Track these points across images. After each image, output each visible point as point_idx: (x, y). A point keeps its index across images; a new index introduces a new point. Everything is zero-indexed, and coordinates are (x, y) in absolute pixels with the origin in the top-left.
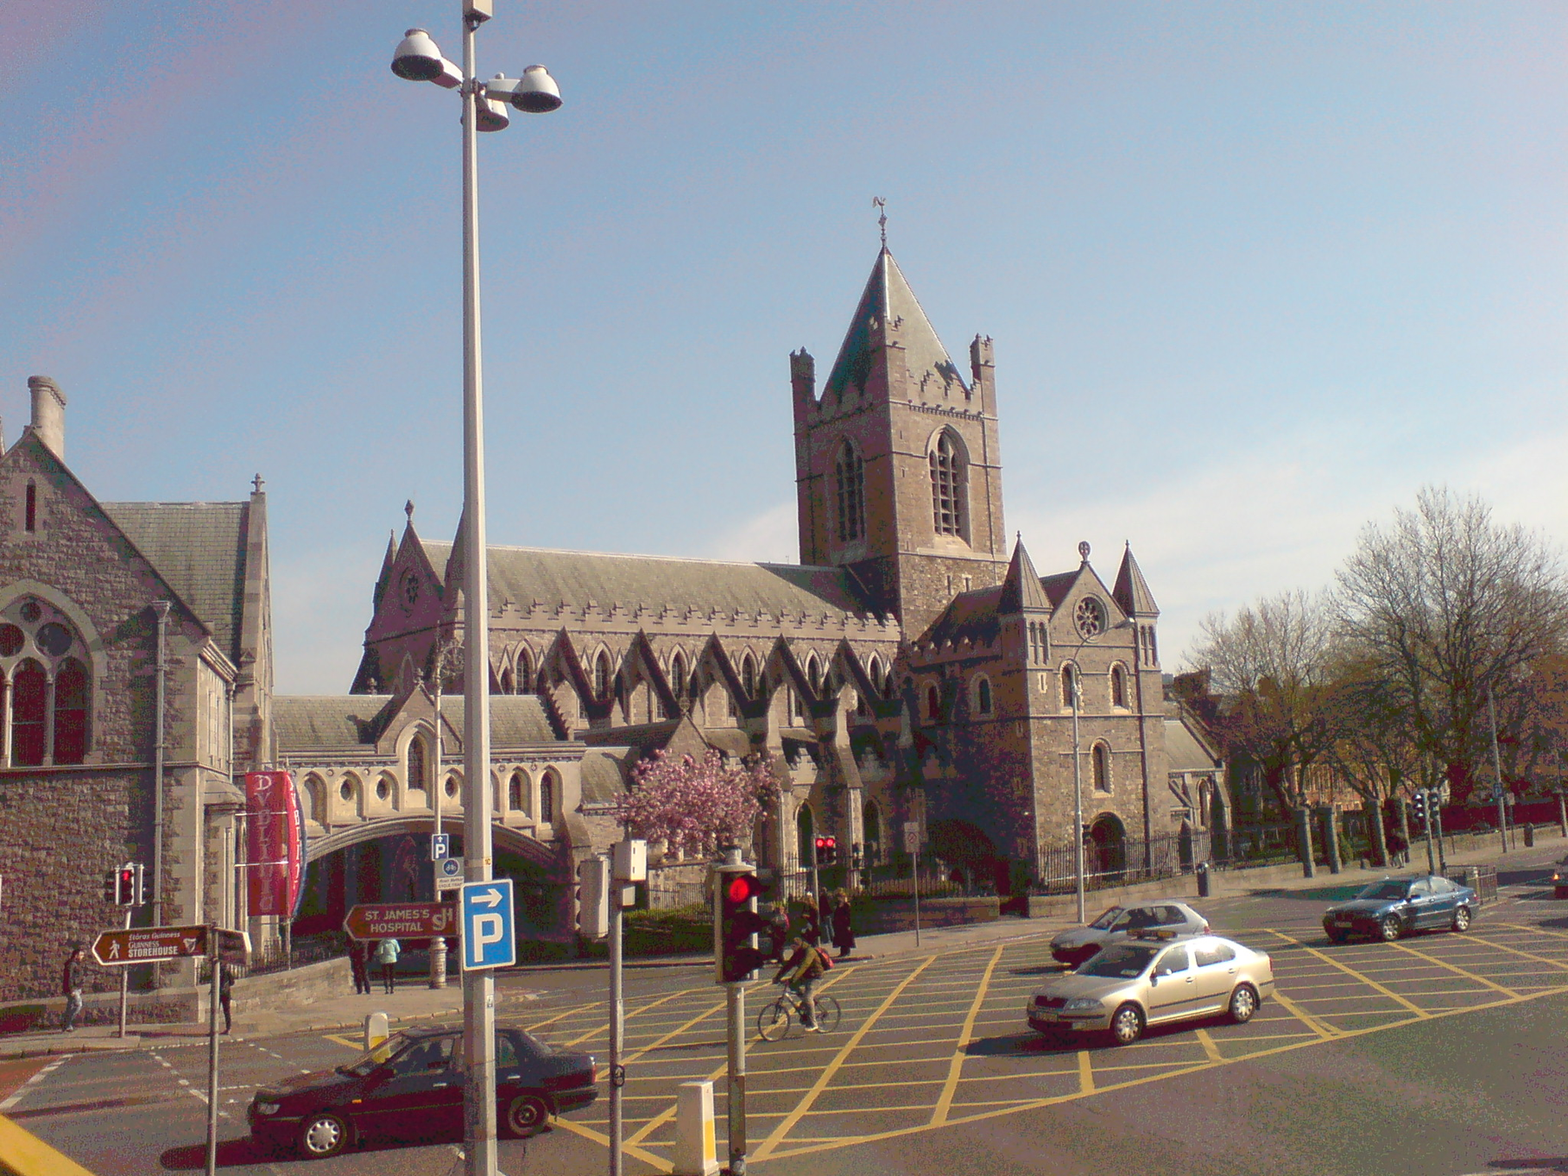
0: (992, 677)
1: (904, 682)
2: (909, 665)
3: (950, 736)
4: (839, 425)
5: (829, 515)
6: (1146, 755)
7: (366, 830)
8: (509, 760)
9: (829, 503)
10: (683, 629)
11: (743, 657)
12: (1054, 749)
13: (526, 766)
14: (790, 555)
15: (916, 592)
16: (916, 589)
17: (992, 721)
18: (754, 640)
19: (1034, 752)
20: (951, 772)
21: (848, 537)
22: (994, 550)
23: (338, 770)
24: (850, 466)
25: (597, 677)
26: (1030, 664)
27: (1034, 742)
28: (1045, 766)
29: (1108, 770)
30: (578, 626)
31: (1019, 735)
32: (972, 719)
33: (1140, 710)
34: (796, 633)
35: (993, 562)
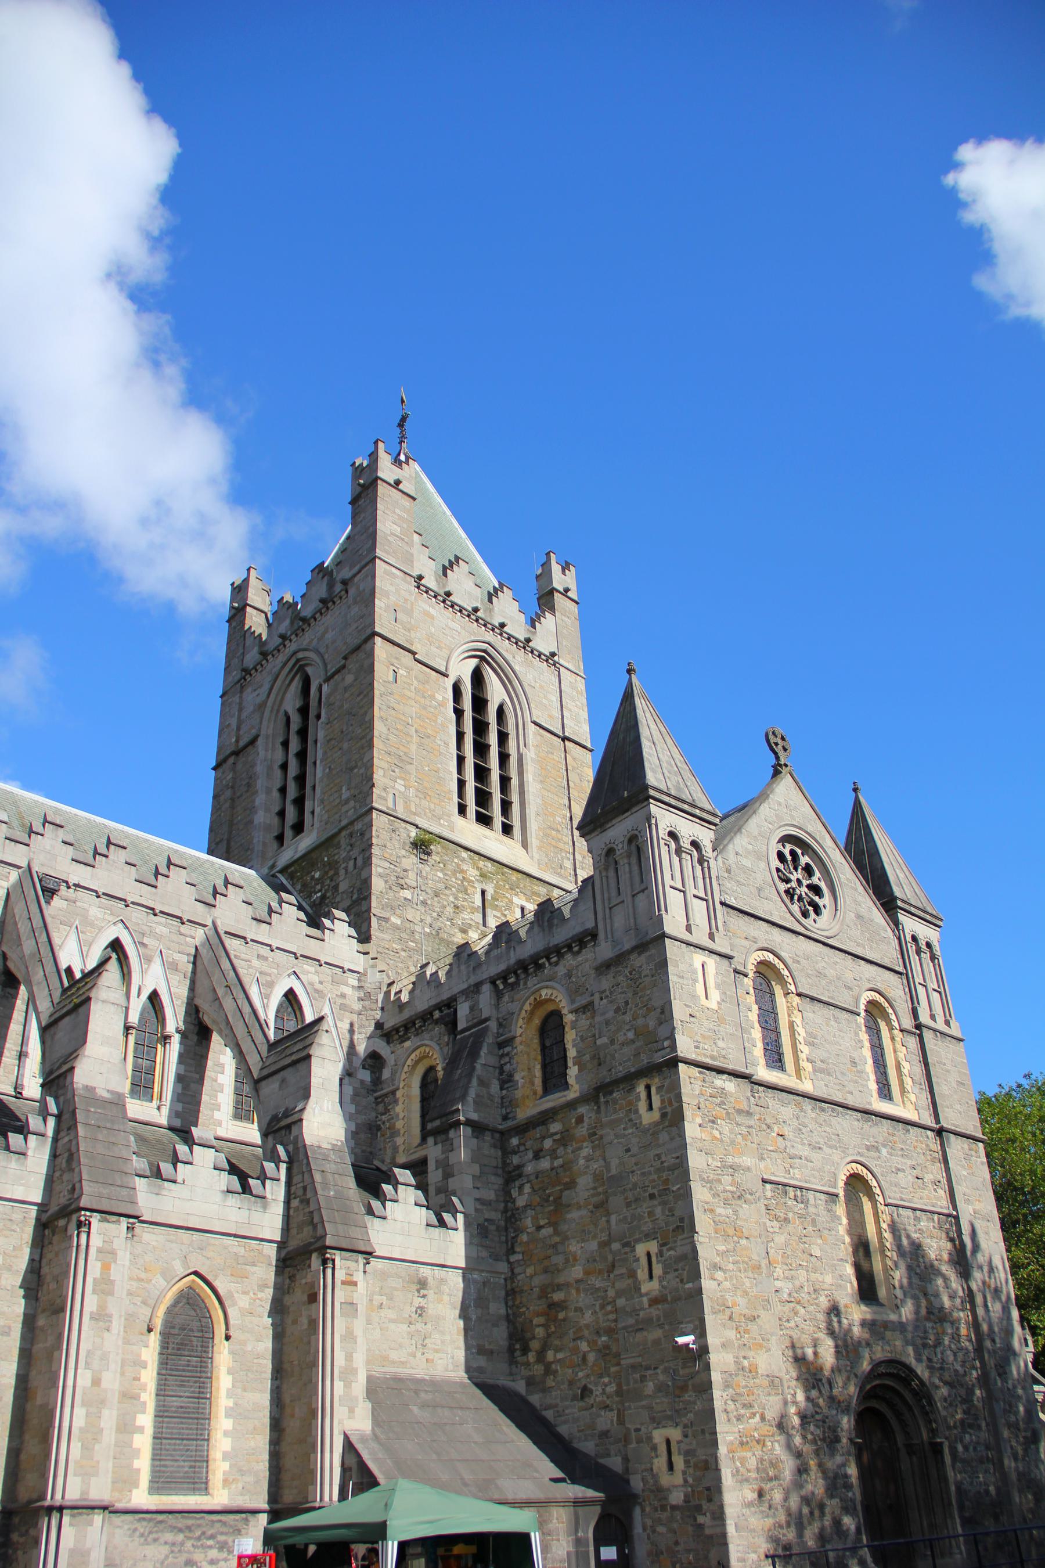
0: (573, 993)
4: (292, 647)
5: (260, 799)
9: (260, 783)
12: (747, 1161)
15: (407, 894)
16: (409, 887)
17: (572, 1105)
19: (695, 1160)
21: (288, 833)
24: (304, 711)
27: (692, 1129)
28: (726, 1203)
31: (648, 1118)
32: (525, 1112)
34: (78, 874)
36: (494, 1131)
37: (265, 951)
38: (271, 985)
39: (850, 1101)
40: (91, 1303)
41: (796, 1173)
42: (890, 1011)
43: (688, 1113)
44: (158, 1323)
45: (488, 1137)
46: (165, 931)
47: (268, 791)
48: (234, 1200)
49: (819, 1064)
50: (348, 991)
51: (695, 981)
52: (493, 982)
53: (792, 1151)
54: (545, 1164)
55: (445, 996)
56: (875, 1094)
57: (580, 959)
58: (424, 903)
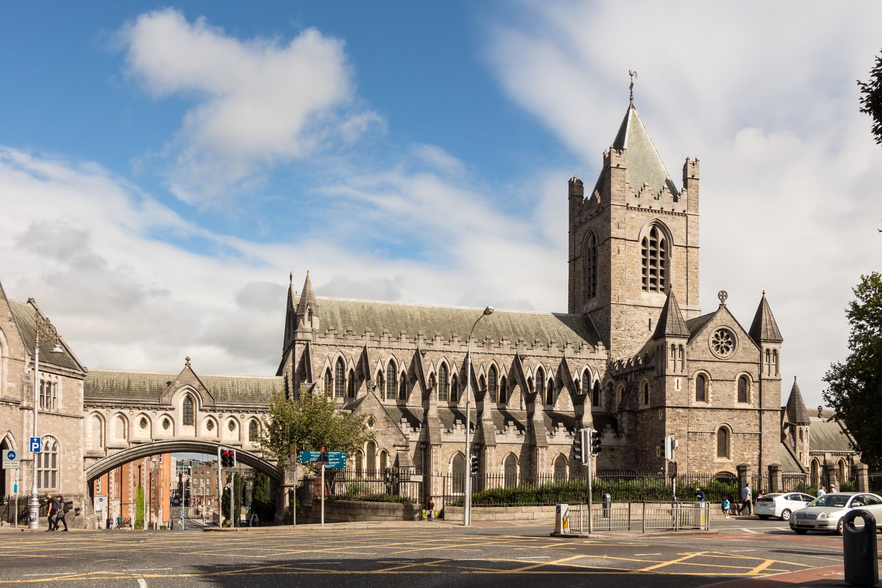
0: (651, 381)
1: (608, 386)
2: (612, 375)
3: (625, 419)
4: (585, 227)
6: (763, 436)
7: (154, 447)
8: (247, 412)
10: (447, 348)
11: (489, 366)
12: (684, 428)
13: (259, 416)
14: (564, 310)
18: (498, 356)
19: (668, 430)
20: (624, 441)
21: (591, 296)
22: (689, 302)
23: (137, 412)
25: (388, 375)
26: (669, 371)
27: (668, 423)
29: (729, 444)
30: (376, 344)
32: (641, 408)
33: (761, 407)
34: (529, 353)
35: (687, 310)
36: (633, 411)
37: (578, 360)
38: (581, 369)
39: (725, 407)
40: (540, 463)
41: (701, 429)
42: (750, 376)
43: (667, 419)
44: (554, 463)
45: (632, 413)
46: (552, 361)
47: (585, 278)
48: (567, 438)
49: (716, 398)
50: (603, 365)
51: (674, 385)
52: (635, 372)
53: (700, 423)
54: (643, 422)
55: (625, 372)
56: (736, 403)
57: (652, 373)
58: (629, 330)
